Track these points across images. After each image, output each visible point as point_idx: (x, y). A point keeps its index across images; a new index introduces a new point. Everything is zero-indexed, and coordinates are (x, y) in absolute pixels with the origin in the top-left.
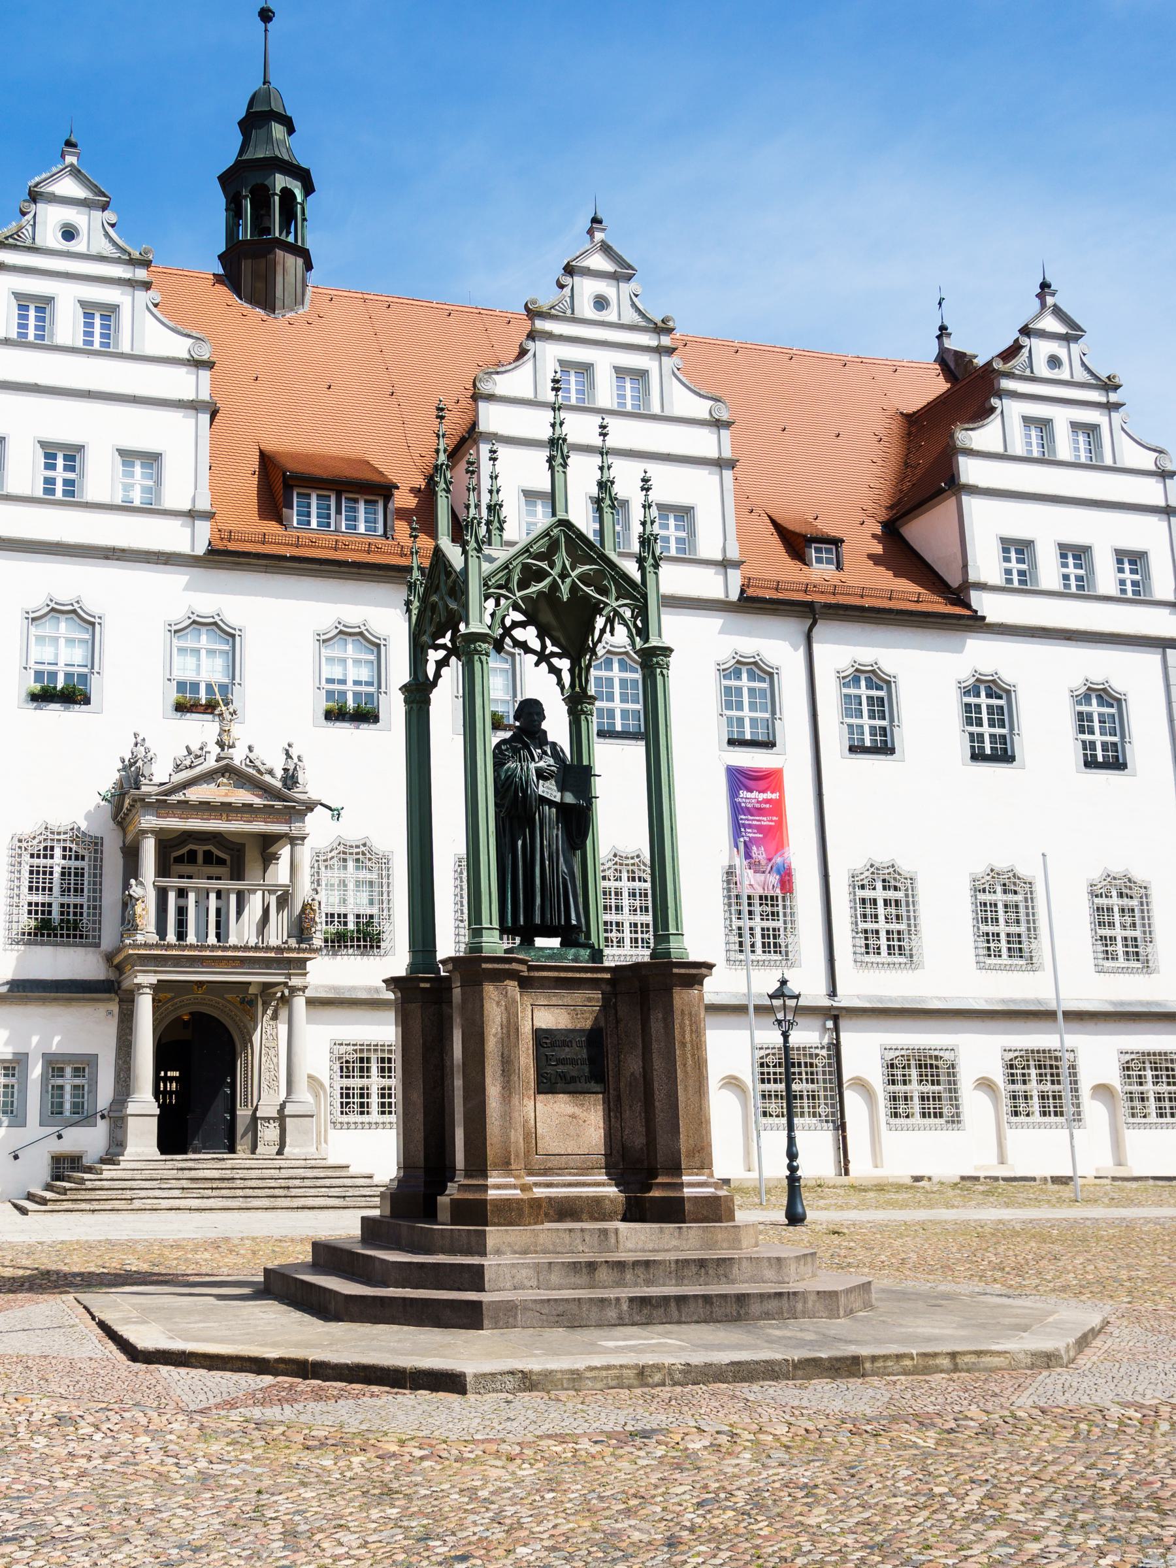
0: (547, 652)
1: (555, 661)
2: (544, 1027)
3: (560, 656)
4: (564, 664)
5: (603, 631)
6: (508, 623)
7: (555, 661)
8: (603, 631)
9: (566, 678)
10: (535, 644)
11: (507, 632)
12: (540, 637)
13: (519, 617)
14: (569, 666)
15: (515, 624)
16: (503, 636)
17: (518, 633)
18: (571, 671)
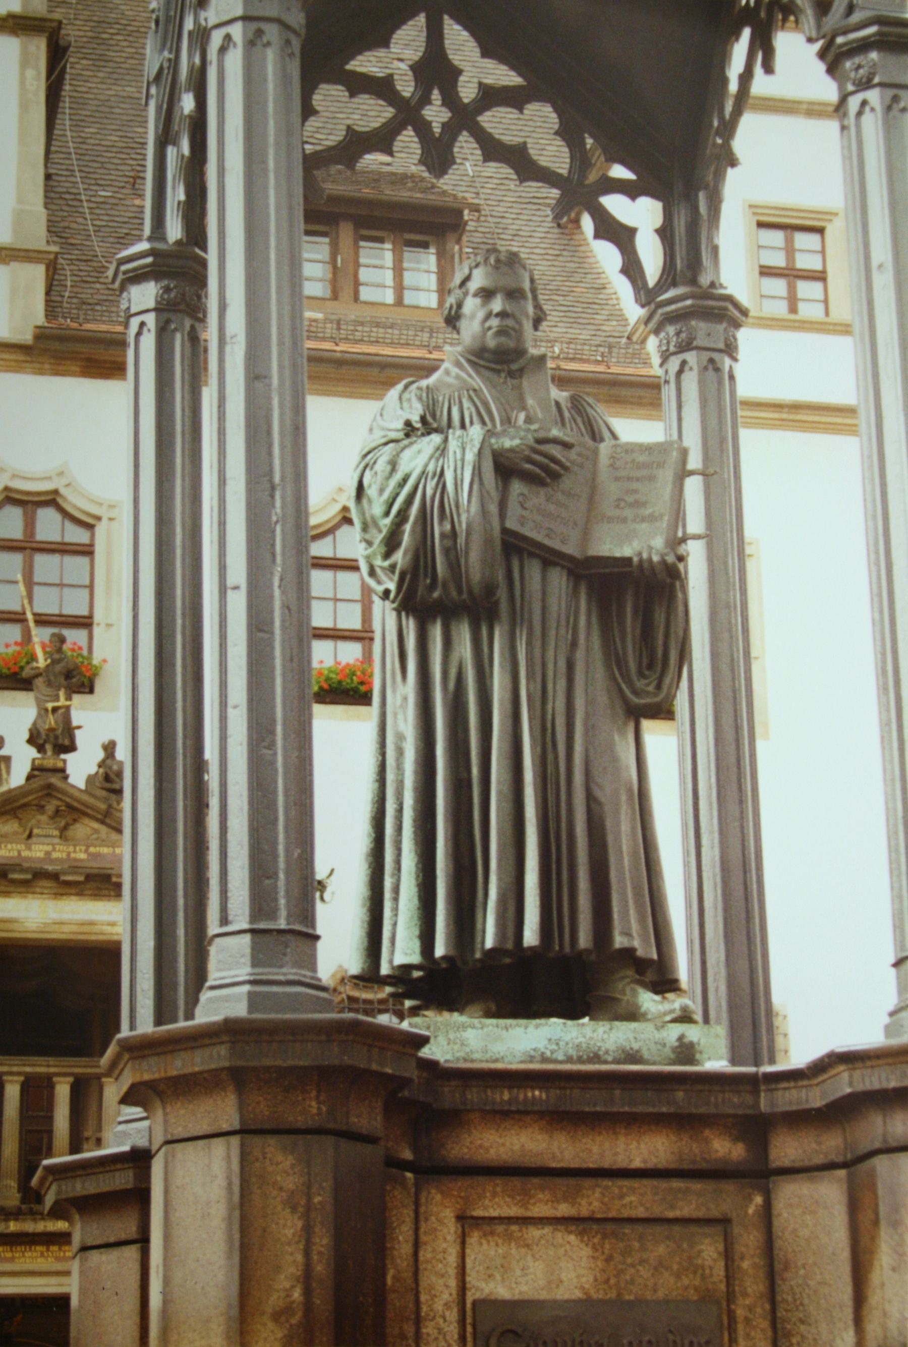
0: (592, 177)
1: (616, 205)
2: (502, 1292)
3: (631, 190)
4: (642, 214)
5: (746, 77)
6: (467, 92)
7: (616, 205)
8: (746, 77)
9: (651, 255)
10: (553, 154)
11: (464, 118)
12: (569, 133)
13: (504, 76)
14: (658, 221)
15: (491, 96)
16: (451, 131)
17: (499, 122)
18: (665, 233)
